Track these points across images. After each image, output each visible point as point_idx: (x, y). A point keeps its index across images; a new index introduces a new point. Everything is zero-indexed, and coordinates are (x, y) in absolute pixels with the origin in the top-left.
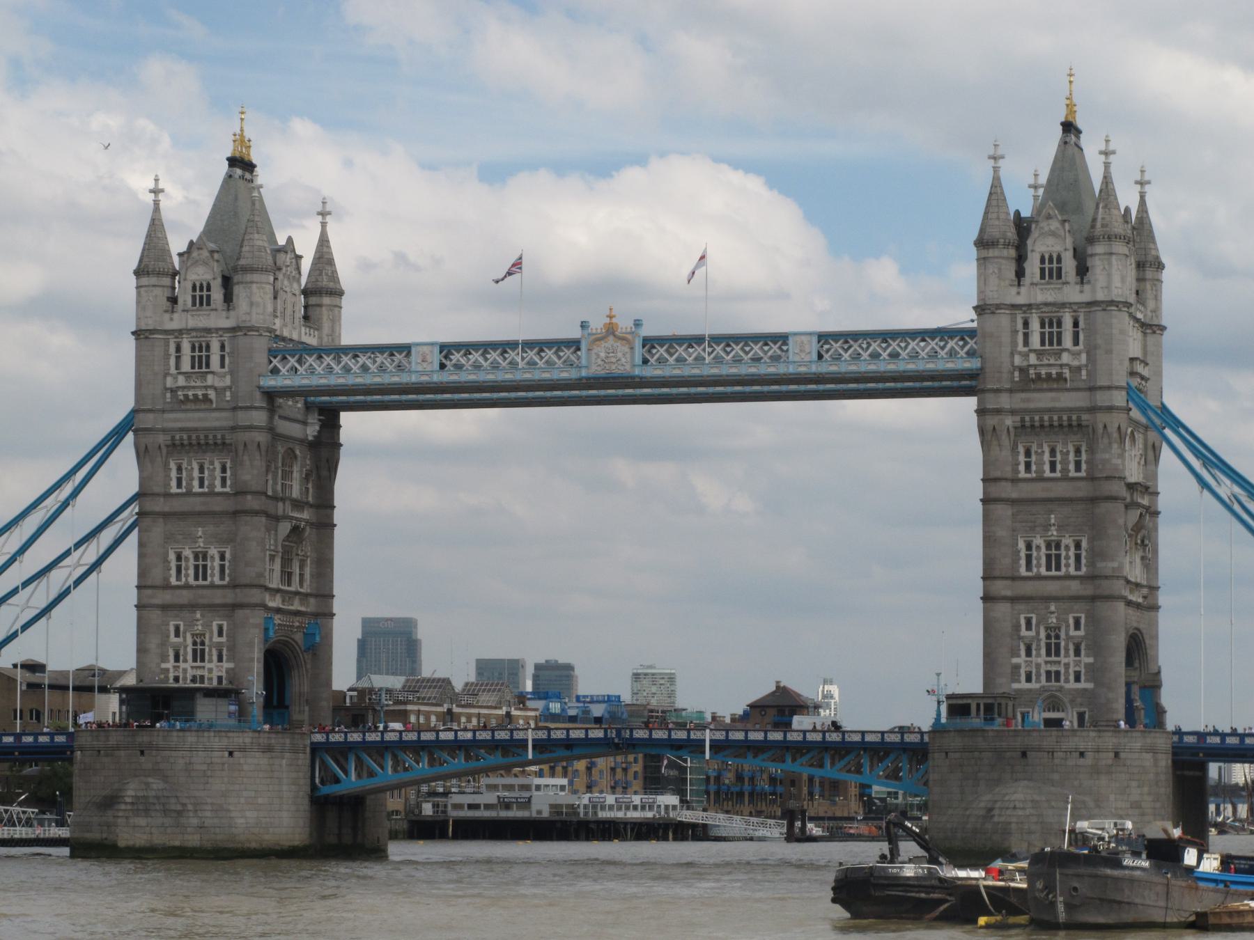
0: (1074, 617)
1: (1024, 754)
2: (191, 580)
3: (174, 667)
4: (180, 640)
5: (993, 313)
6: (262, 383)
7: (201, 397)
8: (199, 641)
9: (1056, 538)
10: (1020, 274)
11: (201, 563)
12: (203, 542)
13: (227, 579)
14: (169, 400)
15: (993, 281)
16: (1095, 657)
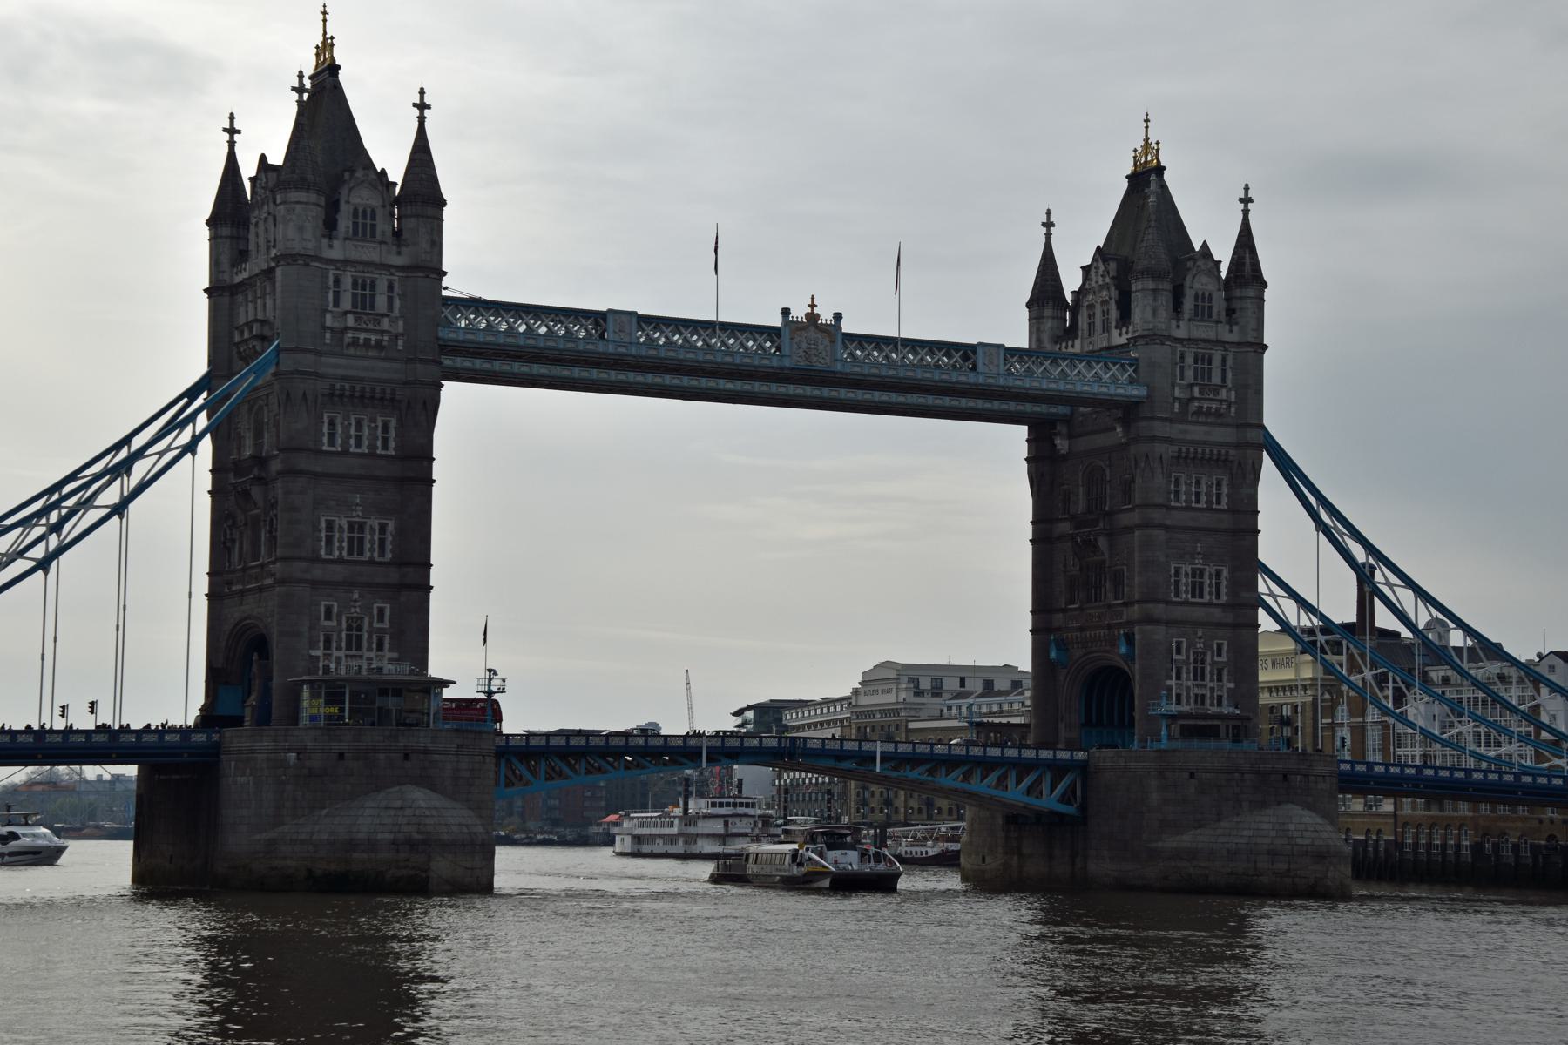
0: (1217, 644)
1: (1285, 776)
2: (346, 558)
3: (324, 655)
4: (334, 623)
5: (1163, 344)
6: (440, 335)
7: (373, 343)
8: (355, 626)
9: (1202, 567)
10: (1177, 306)
11: (356, 535)
12: (362, 511)
13: (389, 556)
14: (328, 342)
15: (1163, 314)
16: (1235, 682)
